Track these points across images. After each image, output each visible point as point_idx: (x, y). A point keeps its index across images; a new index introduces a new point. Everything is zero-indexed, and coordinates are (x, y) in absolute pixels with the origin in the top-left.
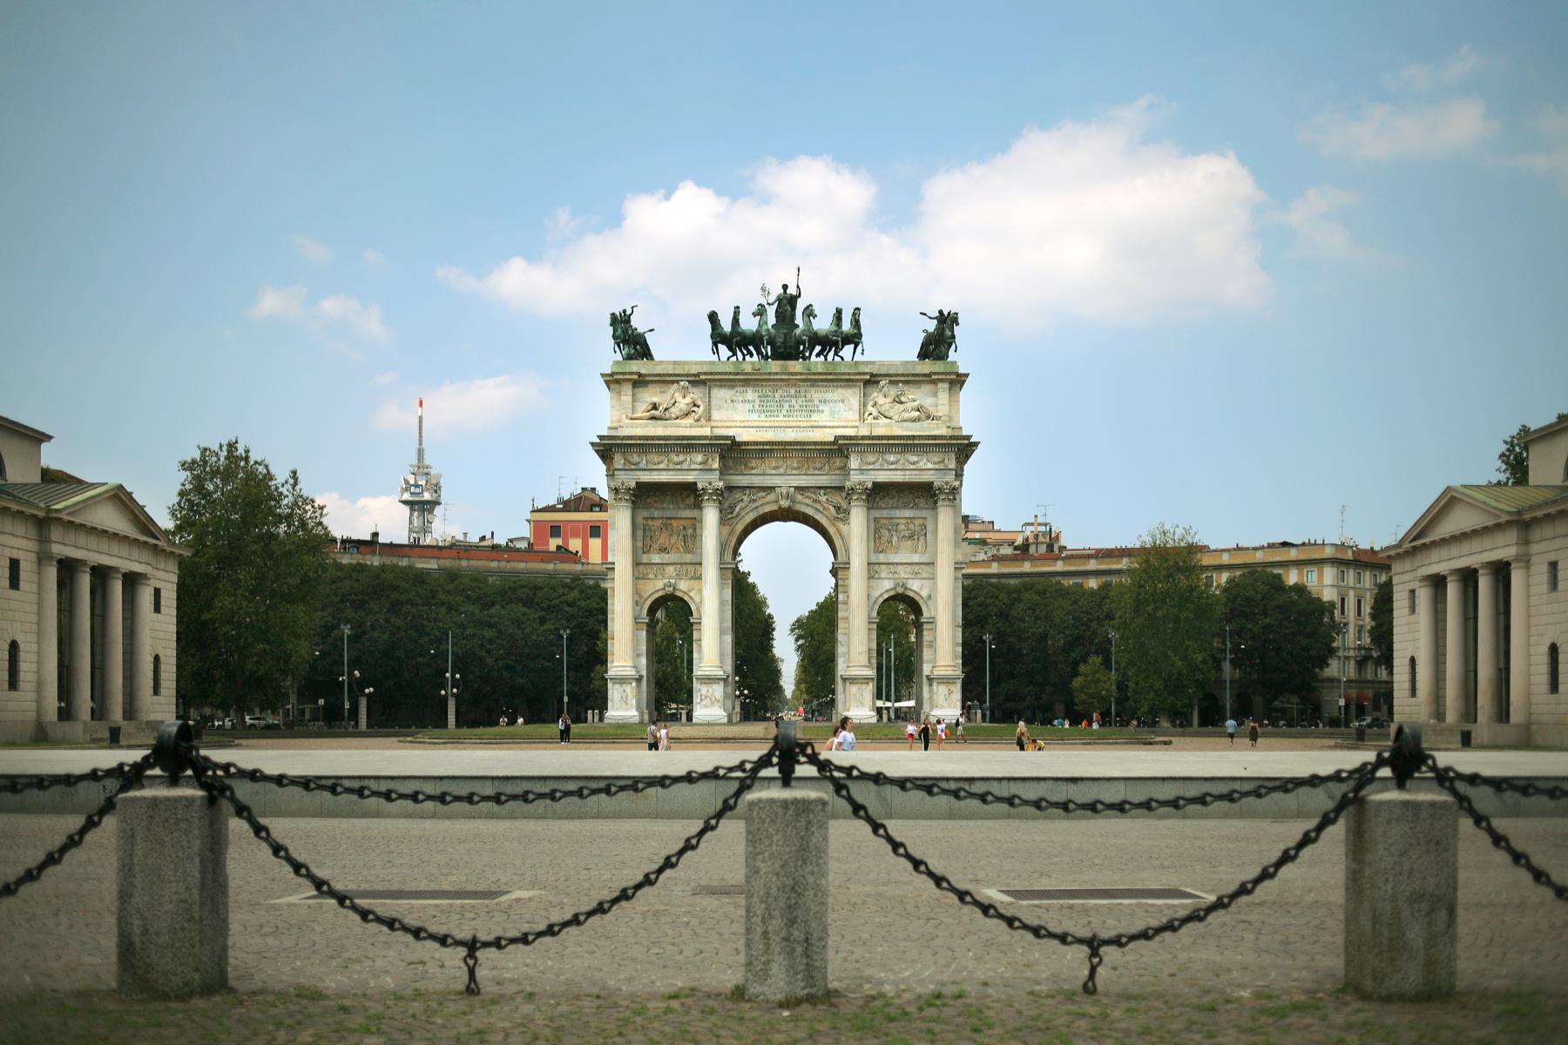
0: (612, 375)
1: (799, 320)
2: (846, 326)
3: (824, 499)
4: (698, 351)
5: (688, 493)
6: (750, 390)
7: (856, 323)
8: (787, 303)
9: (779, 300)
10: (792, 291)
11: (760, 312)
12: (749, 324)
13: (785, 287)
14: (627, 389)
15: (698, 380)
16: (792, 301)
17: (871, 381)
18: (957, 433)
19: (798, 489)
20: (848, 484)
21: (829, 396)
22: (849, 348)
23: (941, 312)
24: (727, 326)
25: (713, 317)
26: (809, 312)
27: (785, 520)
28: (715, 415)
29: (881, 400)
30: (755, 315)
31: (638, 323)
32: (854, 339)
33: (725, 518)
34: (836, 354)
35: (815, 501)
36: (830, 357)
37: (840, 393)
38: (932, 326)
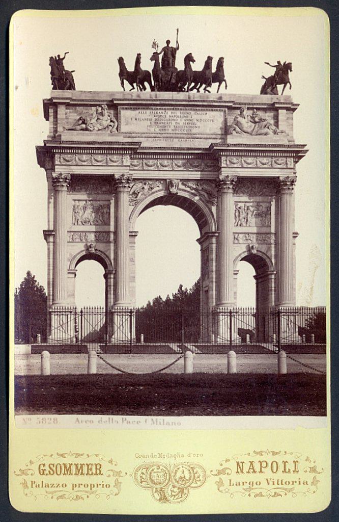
1: (180, 65)
4: (112, 85)
6: (148, 111)
8: (170, 53)
9: (164, 49)
10: (173, 45)
11: (155, 57)
12: (147, 65)
13: (168, 42)
15: (113, 105)
16: (174, 51)
17: (233, 107)
18: (292, 143)
19: (185, 181)
20: (221, 177)
21: (204, 117)
22: (215, 85)
23: (279, 62)
24: (131, 68)
25: (121, 61)
26: (189, 59)
27: (166, 205)
28: (124, 128)
29: (240, 119)
30: (152, 59)
31: (67, 66)
32: (219, 77)
34: (205, 89)
36: (202, 90)
38: (272, 72)
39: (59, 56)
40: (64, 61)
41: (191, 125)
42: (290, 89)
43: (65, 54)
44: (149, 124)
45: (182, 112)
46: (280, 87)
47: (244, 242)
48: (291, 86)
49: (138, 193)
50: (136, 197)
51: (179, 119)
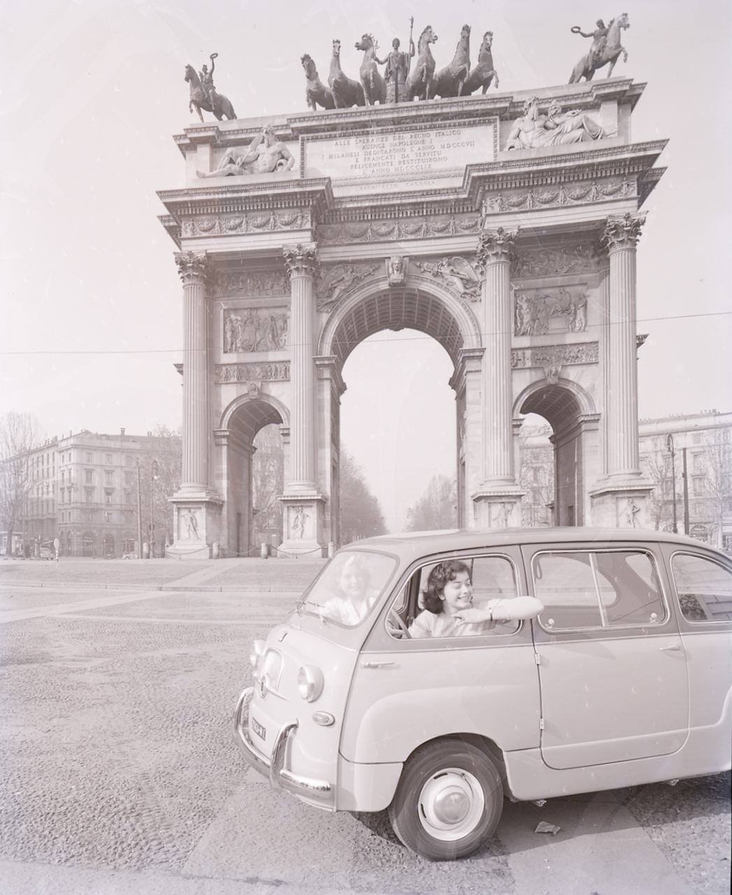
0: (185, 136)
2: (474, 63)
3: (446, 270)
5: (273, 266)
6: (353, 140)
7: (486, 57)
11: (366, 44)
12: (353, 71)
14: (204, 152)
22: (478, 93)
25: (308, 63)
30: (358, 47)
33: (322, 298)
35: (436, 275)
37: (467, 133)
38: (586, 47)
39: (205, 68)
40: (213, 75)
41: (430, 156)
42: (625, 60)
43: (214, 56)
44: (354, 163)
45: (413, 134)
46: (600, 74)
47: (534, 366)
48: (626, 55)
49: (335, 287)
50: (330, 297)
51: (408, 148)
